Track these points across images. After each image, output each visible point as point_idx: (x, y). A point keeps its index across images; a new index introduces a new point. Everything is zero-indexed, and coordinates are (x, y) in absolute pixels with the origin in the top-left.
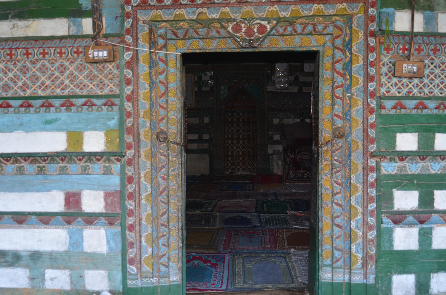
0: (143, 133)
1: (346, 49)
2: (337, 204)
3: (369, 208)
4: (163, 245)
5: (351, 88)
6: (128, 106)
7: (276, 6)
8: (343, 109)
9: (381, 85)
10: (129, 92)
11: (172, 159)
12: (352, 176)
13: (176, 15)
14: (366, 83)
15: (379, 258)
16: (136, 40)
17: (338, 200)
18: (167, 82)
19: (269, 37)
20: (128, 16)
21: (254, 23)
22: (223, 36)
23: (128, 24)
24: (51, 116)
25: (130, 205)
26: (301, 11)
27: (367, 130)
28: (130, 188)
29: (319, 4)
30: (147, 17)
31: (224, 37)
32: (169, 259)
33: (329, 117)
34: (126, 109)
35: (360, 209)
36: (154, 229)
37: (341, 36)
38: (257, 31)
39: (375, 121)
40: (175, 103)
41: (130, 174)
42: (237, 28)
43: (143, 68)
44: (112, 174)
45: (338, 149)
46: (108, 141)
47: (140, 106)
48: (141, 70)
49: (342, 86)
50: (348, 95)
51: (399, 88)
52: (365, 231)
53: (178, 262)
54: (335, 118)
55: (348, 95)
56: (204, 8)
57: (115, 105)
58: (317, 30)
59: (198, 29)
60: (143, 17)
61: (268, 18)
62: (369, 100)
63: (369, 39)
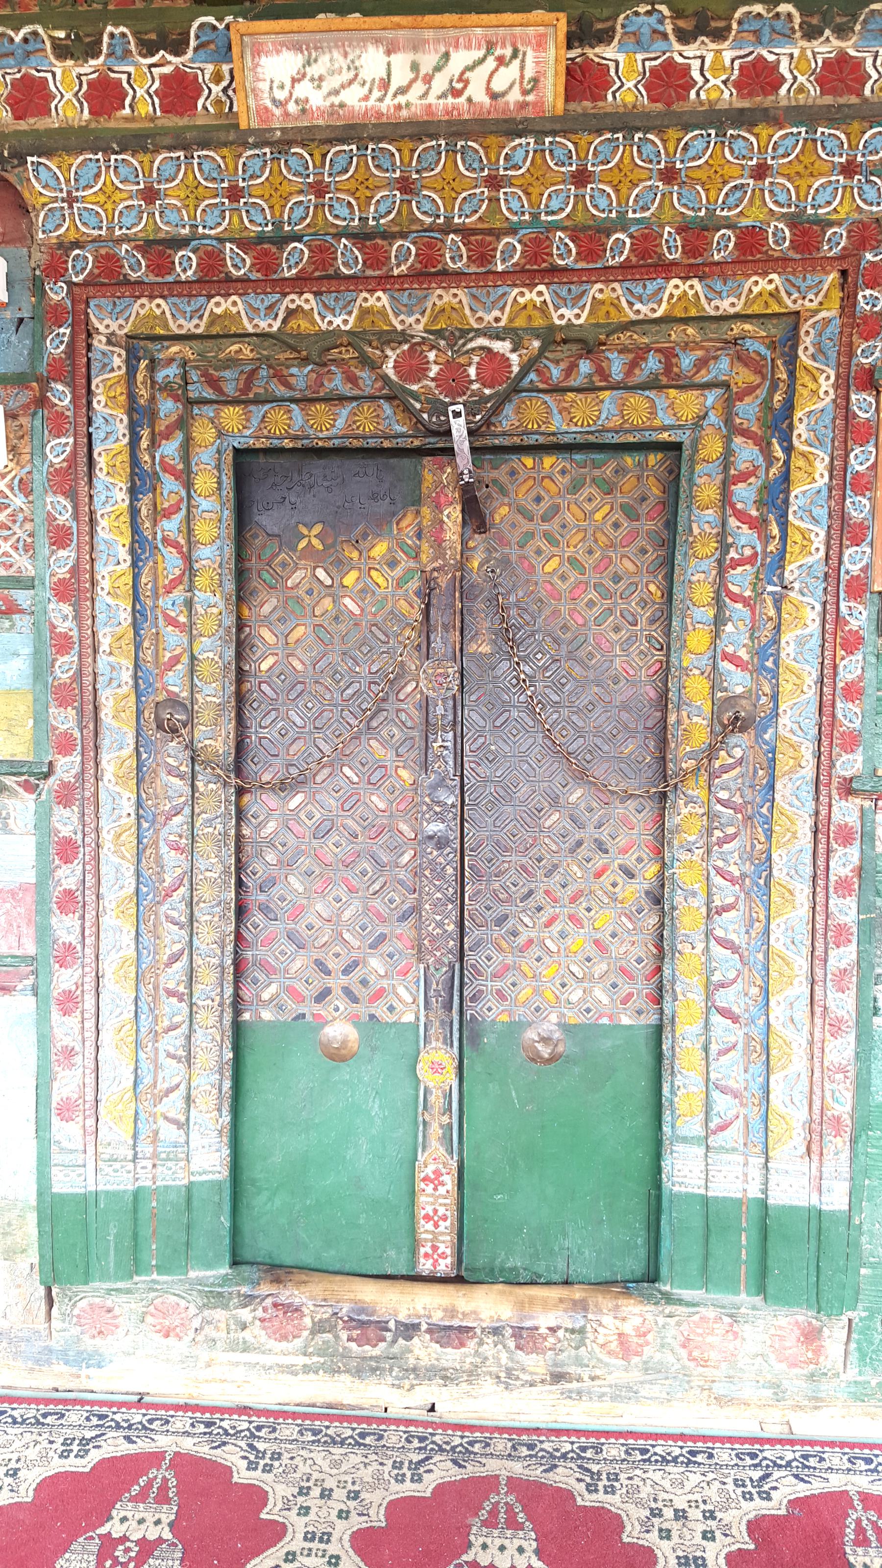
0: (111, 702)
1: (773, 436)
2: (725, 943)
3: (831, 962)
4: (169, 1055)
5: (783, 567)
6: (61, 615)
7: (541, 288)
8: (751, 637)
10: (63, 572)
11: (206, 785)
12: (775, 856)
13: (215, 319)
14: (835, 548)
15: (868, 1127)
17: (726, 930)
18: (189, 542)
19: (516, 399)
20: (56, 315)
21: (469, 346)
22: (368, 391)
23: (56, 344)
25: (65, 927)
26: (624, 304)
27: (833, 705)
28: (68, 876)
29: (685, 278)
30: (121, 321)
31: (372, 398)
32: (189, 1100)
33: (705, 662)
34: (53, 627)
35: (801, 964)
36: (145, 1008)
37: (758, 392)
38: (478, 374)
39: (861, 678)
40: (215, 610)
41: (66, 831)
42: (414, 367)
43: (111, 493)
44: (11, 832)
45: (731, 767)
47: (101, 618)
48: (103, 498)
50: (770, 588)
52: (817, 1035)
53: (219, 1110)
54: (725, 665)
55: (770, 588)
56: (307, 296)
57: (21, 611)
58: (675, 369)
59: (288, 367)
60: (106, 322)
61: (514, 330)
62: (843, 605)
63: (853, 397)
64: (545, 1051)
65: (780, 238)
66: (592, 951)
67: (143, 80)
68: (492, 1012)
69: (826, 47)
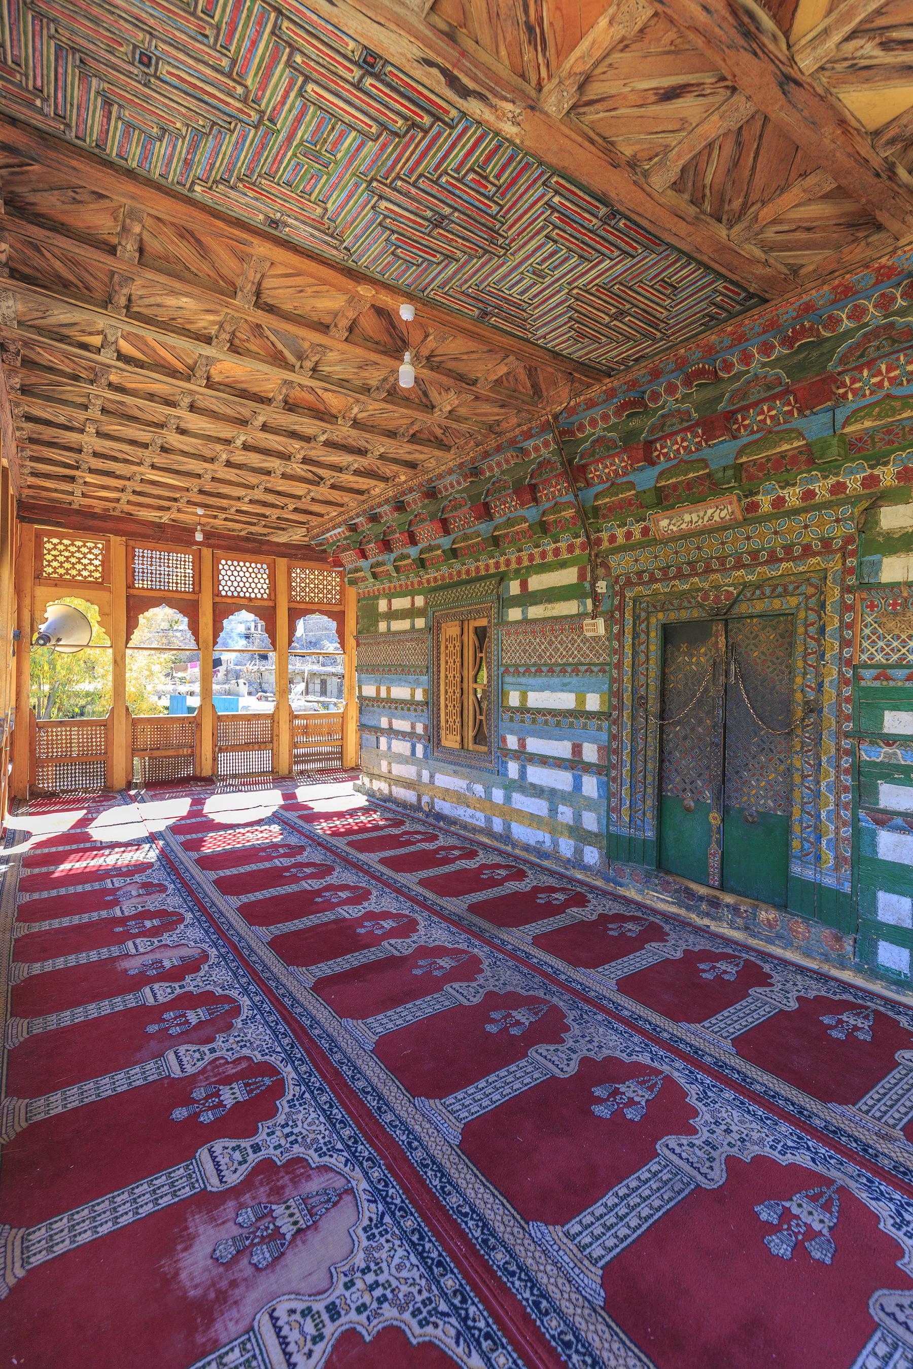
6: (615, 673)
9: (862, 651)
16: (623, 615)
20: (616, 594)
24: (566, 680)
32: (644, 813)
46: (602, 702)
49: (815, 653)
51: (887, 654)
64: (750, 819)
65: (817, 546)
66: (768, 787)
67: (637, 529)
68: (735, 804)
69: (832, 480)
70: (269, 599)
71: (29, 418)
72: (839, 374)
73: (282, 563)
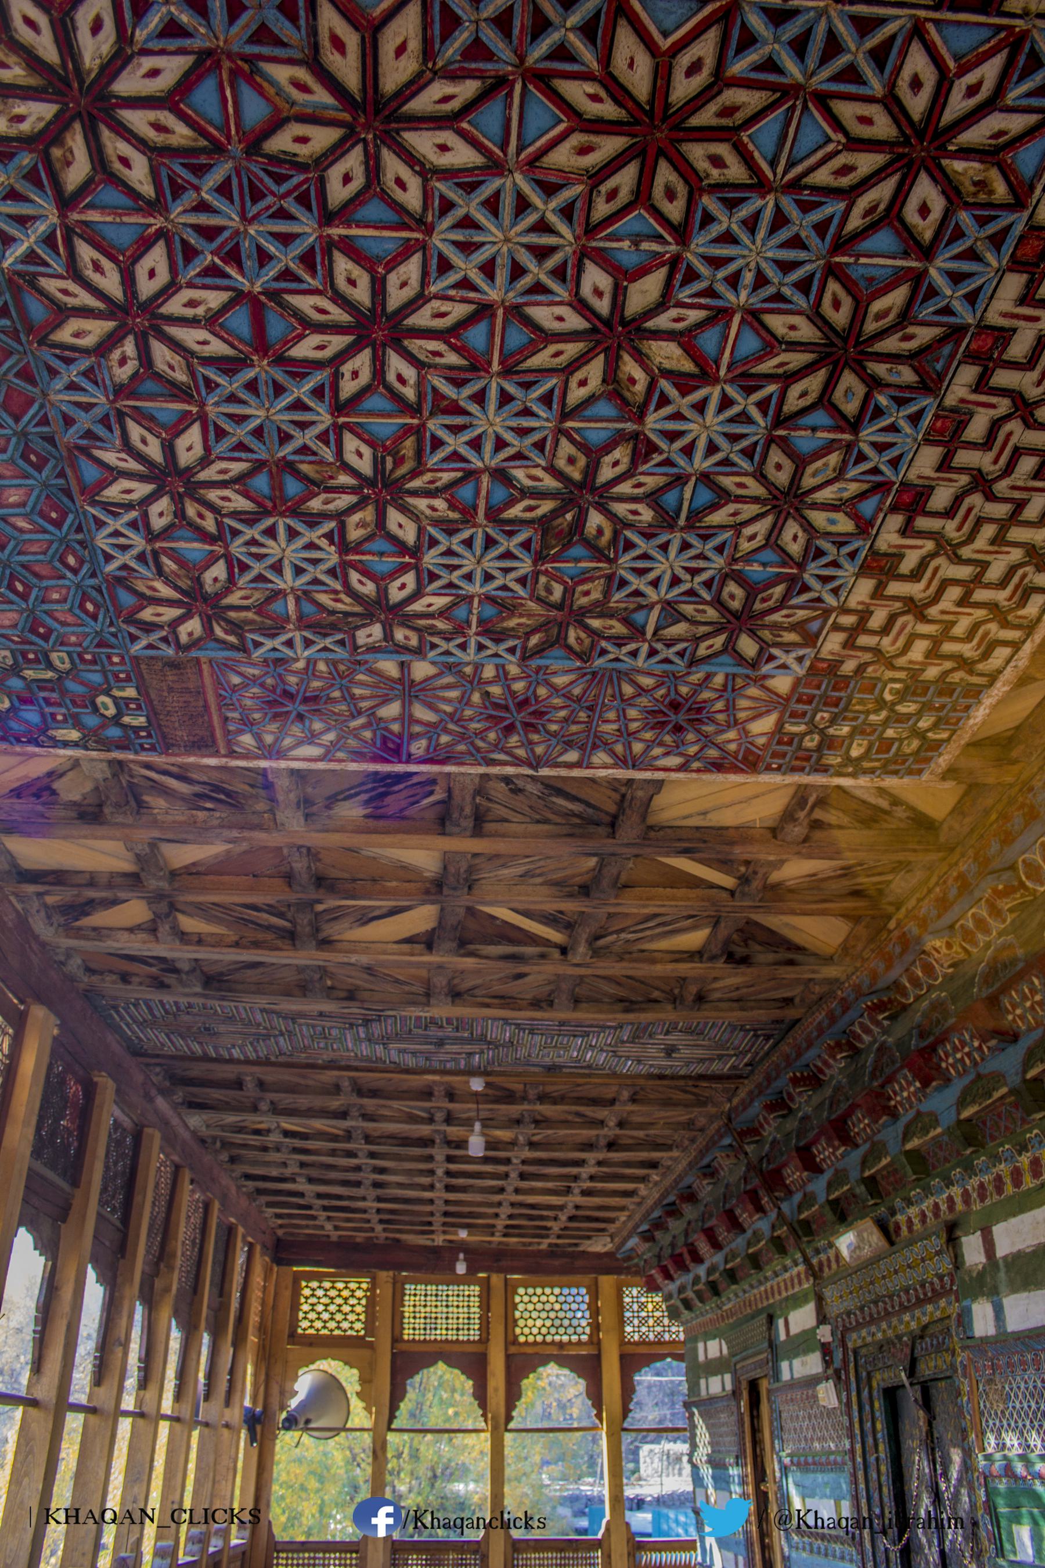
70: (590, 1342)
71: (248, 1177)
72: (882, 1086)
73: (607, 1281)
